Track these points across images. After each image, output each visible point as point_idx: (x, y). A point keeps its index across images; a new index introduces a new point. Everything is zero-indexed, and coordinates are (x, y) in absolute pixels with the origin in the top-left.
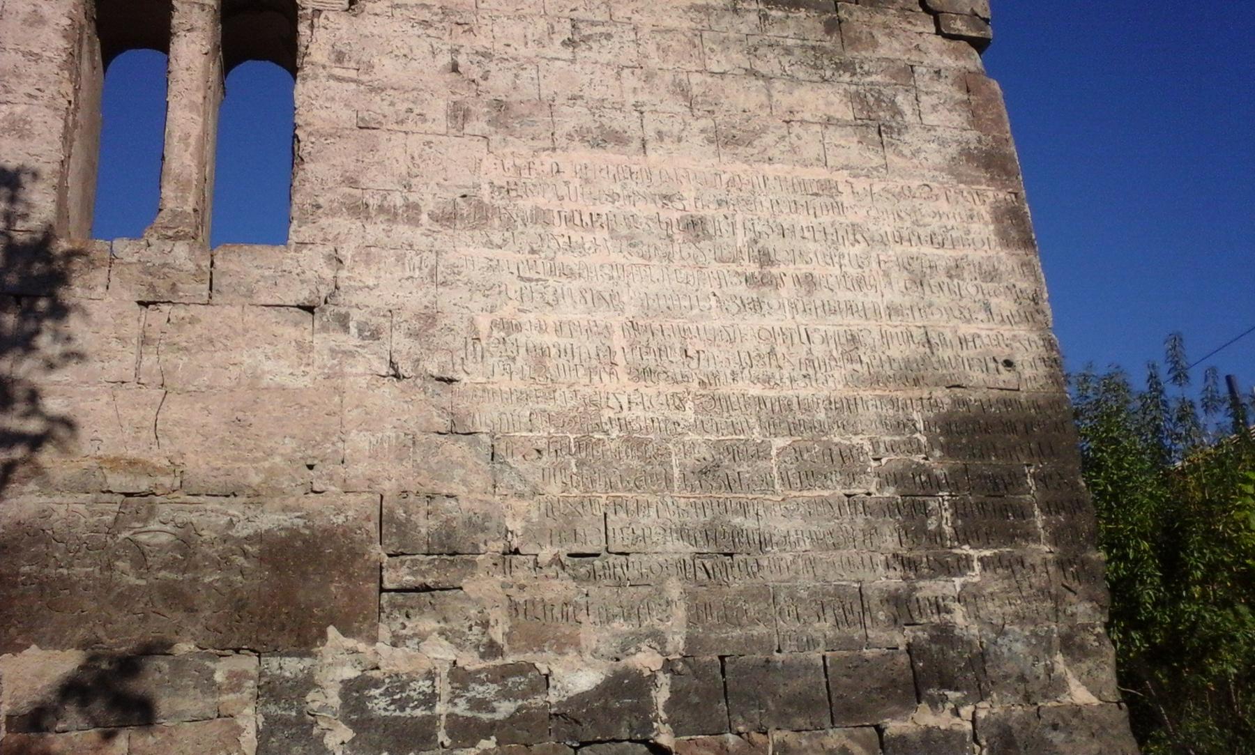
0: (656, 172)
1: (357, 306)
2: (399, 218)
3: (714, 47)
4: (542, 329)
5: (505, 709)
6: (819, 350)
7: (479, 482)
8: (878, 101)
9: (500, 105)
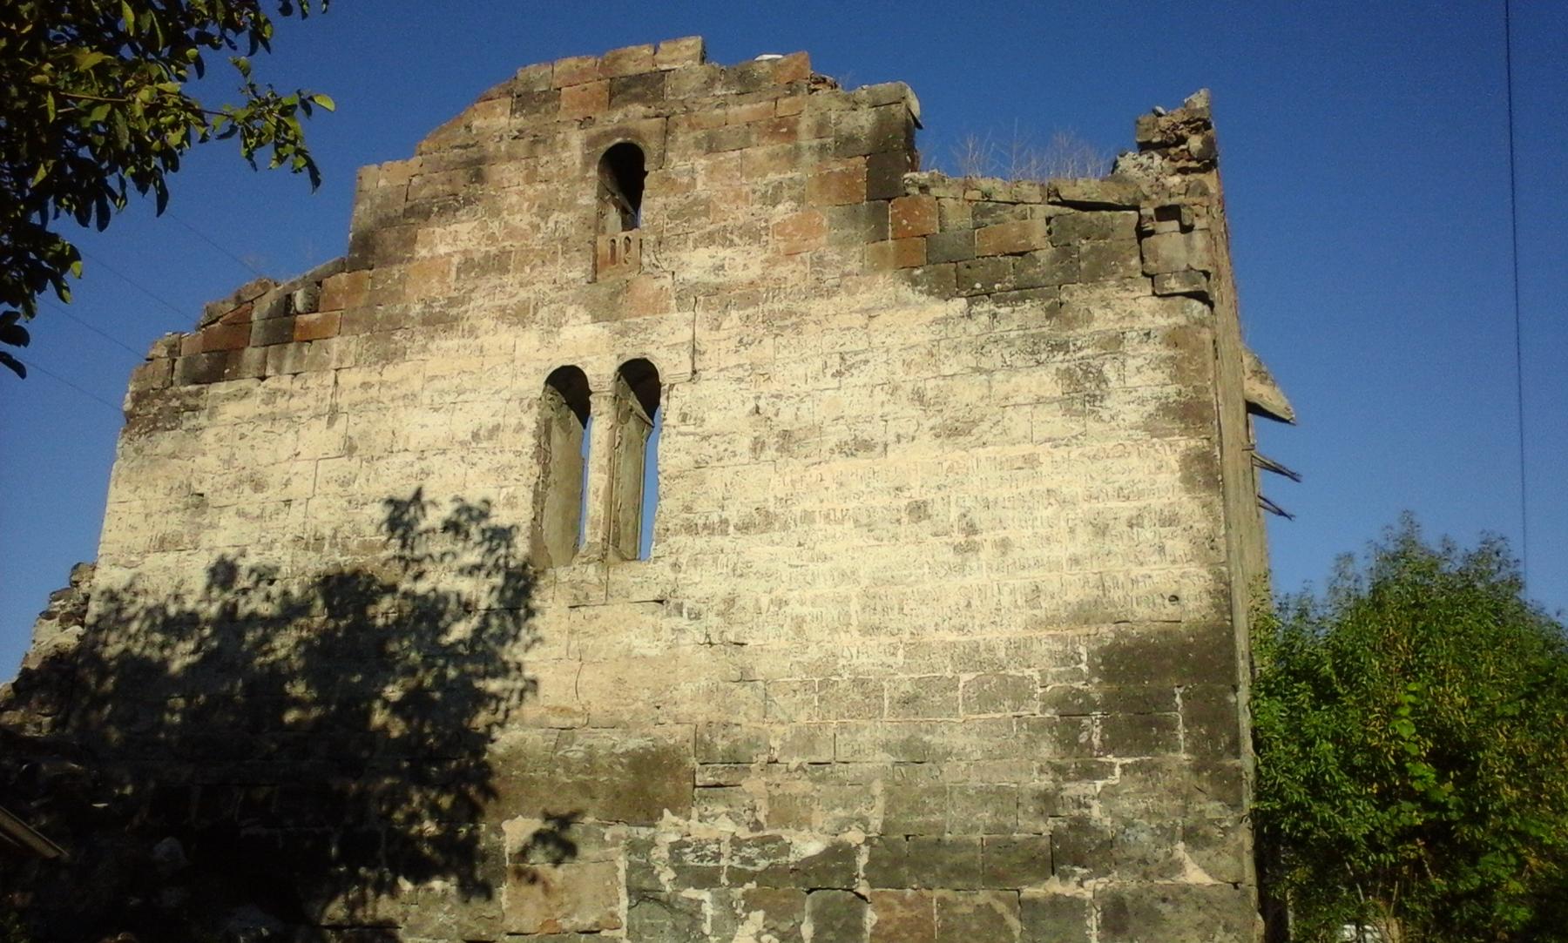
5: (762, 864)
6: (1006, 600)
7: (754, 714)
8: (1086, 373)
9: (786, 435)
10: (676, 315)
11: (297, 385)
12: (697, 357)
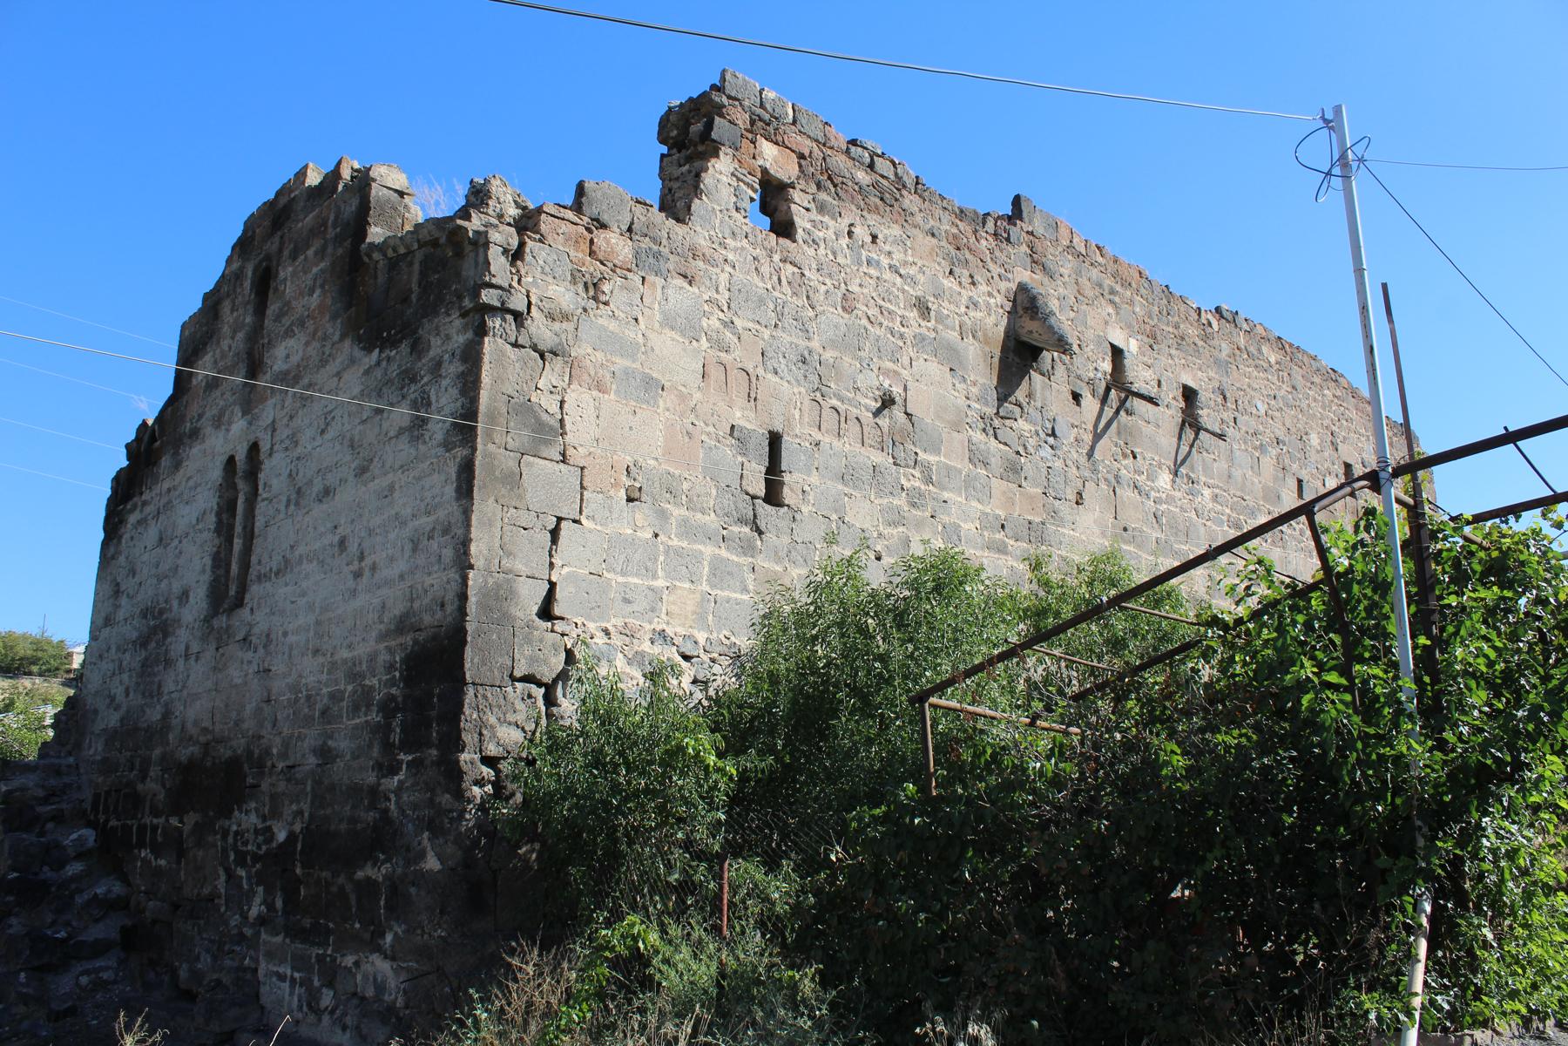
5: (264, 848)
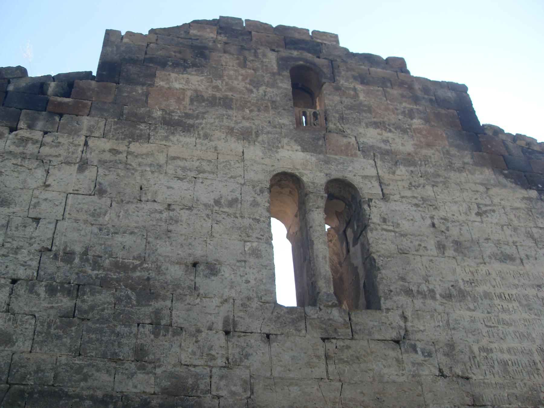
0: (530, 274)
1: (418, 340)
2: (427, 296)
3: (538, 216)
4: (501, 351)
9: (457, 244)
10: (364, 160)
11: (48, 139)
12: (384, 187)
